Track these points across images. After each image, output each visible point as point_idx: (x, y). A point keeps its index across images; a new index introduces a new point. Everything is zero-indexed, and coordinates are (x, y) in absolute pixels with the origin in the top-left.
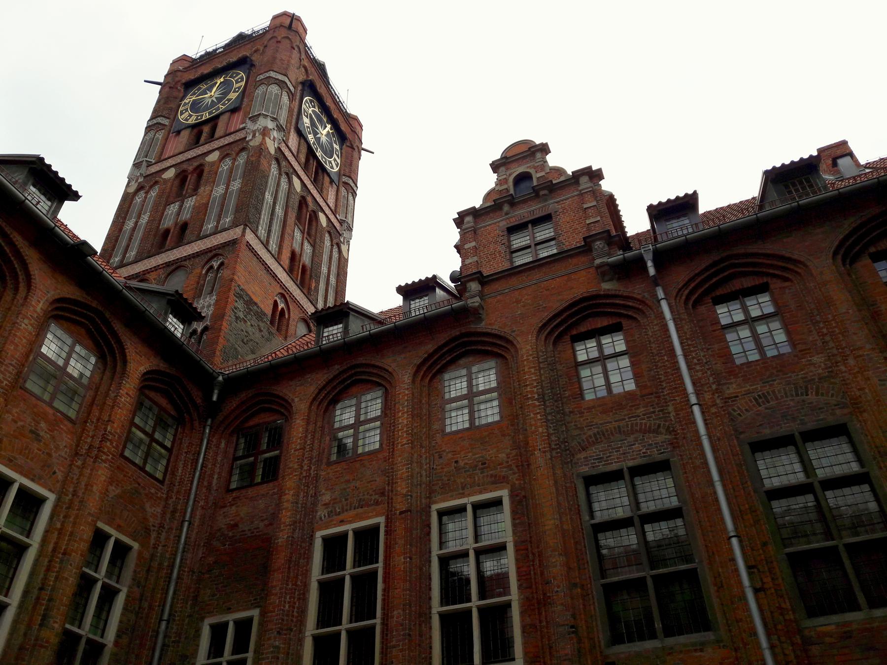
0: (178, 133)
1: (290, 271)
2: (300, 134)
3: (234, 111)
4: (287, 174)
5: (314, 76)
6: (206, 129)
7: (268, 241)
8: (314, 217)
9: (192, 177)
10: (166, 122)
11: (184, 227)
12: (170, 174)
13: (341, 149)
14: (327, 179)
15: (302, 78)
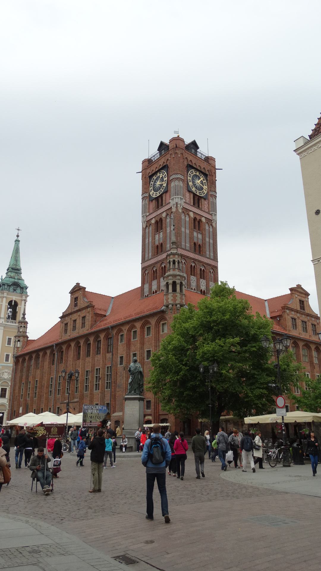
0: (152, 201)
1: (195, 252)
2: (190, 191)
3: (166, 192)
4: (188, 214)
5: (190, 158)
6: (160, 200)
7: (186, 246)
8: (200, 220)
9: (159, 225)
10: (147, 195)
11: (162, 244)
12: (153, 221)
13: (207, 180)
14: (203, 200)
15: (186, 163)
